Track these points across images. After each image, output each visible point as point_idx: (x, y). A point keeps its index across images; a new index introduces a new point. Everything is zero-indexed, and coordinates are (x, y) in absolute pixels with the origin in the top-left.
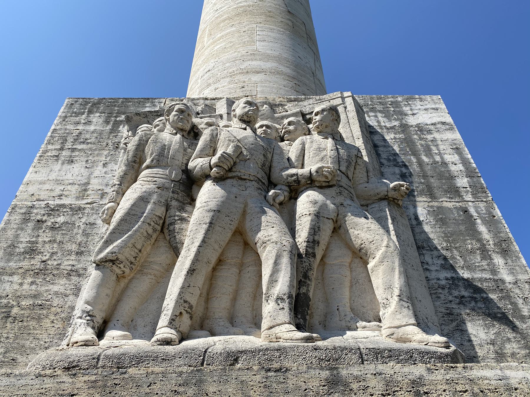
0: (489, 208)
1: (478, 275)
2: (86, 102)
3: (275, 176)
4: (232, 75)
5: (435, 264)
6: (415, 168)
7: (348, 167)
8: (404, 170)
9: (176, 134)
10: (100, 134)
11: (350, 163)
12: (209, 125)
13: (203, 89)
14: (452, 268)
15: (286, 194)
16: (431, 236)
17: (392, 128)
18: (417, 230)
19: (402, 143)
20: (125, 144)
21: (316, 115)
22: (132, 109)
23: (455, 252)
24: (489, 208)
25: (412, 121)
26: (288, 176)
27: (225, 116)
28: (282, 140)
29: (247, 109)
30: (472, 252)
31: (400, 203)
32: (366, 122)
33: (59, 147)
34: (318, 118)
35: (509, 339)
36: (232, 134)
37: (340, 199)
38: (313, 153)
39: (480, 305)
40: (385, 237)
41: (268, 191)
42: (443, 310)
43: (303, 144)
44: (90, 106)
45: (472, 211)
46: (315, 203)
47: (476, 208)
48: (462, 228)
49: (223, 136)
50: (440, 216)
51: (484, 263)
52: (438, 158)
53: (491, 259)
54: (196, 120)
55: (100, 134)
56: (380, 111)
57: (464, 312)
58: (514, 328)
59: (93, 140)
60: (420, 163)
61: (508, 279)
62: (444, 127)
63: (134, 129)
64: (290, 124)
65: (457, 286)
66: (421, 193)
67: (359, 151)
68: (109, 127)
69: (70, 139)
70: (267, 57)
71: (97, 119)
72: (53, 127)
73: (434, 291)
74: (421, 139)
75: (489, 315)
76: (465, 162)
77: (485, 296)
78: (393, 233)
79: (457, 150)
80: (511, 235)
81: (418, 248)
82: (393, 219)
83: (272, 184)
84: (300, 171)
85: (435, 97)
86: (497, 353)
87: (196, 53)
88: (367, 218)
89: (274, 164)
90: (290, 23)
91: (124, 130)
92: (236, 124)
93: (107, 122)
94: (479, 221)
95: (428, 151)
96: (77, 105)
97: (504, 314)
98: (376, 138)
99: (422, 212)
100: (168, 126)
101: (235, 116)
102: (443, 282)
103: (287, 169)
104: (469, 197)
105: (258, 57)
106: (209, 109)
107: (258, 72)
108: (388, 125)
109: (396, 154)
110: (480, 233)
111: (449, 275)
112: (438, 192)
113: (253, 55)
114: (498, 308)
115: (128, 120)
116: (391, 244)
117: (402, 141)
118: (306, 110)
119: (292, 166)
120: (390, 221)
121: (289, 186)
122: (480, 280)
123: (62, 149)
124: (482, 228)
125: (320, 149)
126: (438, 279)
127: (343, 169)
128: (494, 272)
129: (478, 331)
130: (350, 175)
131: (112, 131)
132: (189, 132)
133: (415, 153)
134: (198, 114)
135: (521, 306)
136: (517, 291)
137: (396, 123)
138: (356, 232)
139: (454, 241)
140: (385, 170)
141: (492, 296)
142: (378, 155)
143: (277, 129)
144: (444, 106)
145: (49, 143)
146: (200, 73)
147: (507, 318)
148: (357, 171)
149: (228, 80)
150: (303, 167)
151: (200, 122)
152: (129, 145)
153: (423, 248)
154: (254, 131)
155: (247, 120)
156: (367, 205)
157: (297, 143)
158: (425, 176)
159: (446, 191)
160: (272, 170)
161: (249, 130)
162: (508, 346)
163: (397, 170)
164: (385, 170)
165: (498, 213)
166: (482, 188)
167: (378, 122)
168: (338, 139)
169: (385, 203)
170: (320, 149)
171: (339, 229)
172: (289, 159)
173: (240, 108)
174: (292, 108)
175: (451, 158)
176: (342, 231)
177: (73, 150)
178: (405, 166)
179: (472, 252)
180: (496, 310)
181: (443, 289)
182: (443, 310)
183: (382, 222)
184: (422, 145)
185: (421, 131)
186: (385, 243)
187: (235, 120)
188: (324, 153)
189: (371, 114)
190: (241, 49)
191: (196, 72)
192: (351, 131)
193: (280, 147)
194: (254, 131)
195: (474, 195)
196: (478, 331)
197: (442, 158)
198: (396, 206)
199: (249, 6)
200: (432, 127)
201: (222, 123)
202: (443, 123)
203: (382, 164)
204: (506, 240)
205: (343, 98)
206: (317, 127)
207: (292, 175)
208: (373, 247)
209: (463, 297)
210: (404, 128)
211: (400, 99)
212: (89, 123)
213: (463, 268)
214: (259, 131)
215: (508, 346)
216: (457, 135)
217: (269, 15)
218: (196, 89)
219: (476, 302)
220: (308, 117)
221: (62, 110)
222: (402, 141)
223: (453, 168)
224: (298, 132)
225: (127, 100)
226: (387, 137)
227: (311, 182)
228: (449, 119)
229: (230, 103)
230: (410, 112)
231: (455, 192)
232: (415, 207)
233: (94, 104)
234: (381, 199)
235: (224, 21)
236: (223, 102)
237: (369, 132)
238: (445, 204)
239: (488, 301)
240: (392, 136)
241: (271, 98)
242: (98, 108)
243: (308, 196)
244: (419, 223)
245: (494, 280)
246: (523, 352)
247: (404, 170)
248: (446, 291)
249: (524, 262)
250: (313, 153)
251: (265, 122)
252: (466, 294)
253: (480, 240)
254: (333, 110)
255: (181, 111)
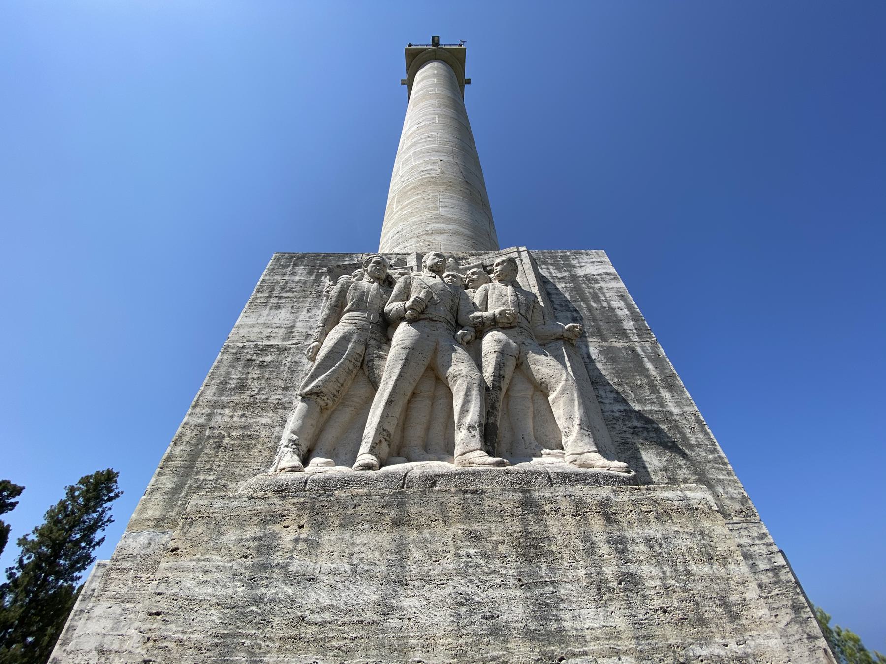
0: (654, 348)
1: (648, 408)
2: (291, 256)
3: (461, 320)
4: (418, 235)
5: (609, 398)
6: (585, 312)
7: (527, 311)
8: (575, 314)
9: (373, 282)
10: (305, 284)
11: (528, 308)
12: (402, 274)
13: (393, 248)
14: (625, 401)
15: (472, 334)
16: (604, 372)
17: (562, 278)
18: (590, 367)
19: (572, 291)
20: (327, 292)
21: (497, 265)
22: (333, 263)
23: (626, 387)
24: (654, 348)
25: (580, 272)
26: (474, 318)
27: (415, 268)
28: (467, 288)
29: (436, 261)
30: (642, 387)
31: (574, 342)
32: (539, 273)
33: (267, 295)
34: (499, 268)
35: (680, 466)
36: (423, 281)
37: (521, 339)
38: (495, 298)
39: (652, 434)
40: (564, 372)
41: (457, 332)
42: (619, 440)
43: (486, 291)
44: (295, 260)
45: (639, 350)
46: (499, 341)
47: (642, 347)
48: (631, 365)
49: (415, 284)
50: (610, 355)
51: (653, 397)
52: (605, 304)
53: (659, 393)
54: (390, 271)
55: (305, 284)
56: (551, 264)
57: (638, 441)
58: (684, 456)
59: (298, 289)
60: (589, 308)
61: (676, 411)
62: (609, 277)
63: (335, 280)
64: (473, 274)
65: (631, 417)
66: (592, 335)
67: (536, 296)
68: (313, 278)
69: (277, 288)
70: (447, 220)
71: (301, 273)
72: (262, 278)
73: (610, 422)
74: (589, 287)
75: (660, 444)
76: (629, 307)
77: (656, 426)
78: (569, 369)
79: (622, 297)
80: (675, 372)
81: (592, 383)
82: (569, 357)
83: (459, 326)
84: (485, 314)
85: (599, 252)
86: (669, 478)
87: (386, 217)
88: (546, 355)
89: (461, 308)
90: (468, 192)
91: (326, 281)
92: (426, 274)
93: (310, 274)
94: (646, 359)
95: (596, 299)
96: (283, 259)
97: (674, 442)
98: (549, 287)
99: (593, 351)
100: (366, 276)
101: (425, 266)
102: (617, 414)
103: (473, 312)
104: (635, 338)
105: (441, 221)
106: (401, 262)
107: (441, 233)
108: (559, 276)
109: (567, 301)
110: (648, 370)
111: (622, 408)
112: (607, 334)
113: (438, 219)
114: (668, 437)
115: (330, 272)
116: (570, 378)
117: (571, 290)
118: (487, 262)
119: (476, 309)
120: (566, 358)
121: (475, 328)
122: (651, 412)
123: (270, 297)
124: (649, 366)
125: (501, 295)
126: (613, 411)
127: (523, 312)
128: (663, 404)
129: (651, 458)
130: (529, 317)
131: (315, 281)
132: (385, 281)
133: (585, 300)
134: (391, 266)
135: (689, 435)
136: (684, 422)
137: (566, 274)
138: (537, 368)
139: (625, 377)
140: (558, 314)
141: (662, 427)
142: (552, 302)
143: (462, 279)
144: (608, 259)
145: (258, 291)
146: (390, 234)
147: (677, 447)
148: (535, 315)
149: (415, 239)
150: (486, 310)
151: (394, 272)
152: (331, 293)
153: (597, 383)
154: (442, 279)
155: (436, 270)
156: (548, 343)
157: (481, 289)
158: (594, 320)
159: (614, 333)
160: (459, 313)
161: (438, 278)
162: (679, 472)
163: (569, 315)
164: (558, 314)
165: (662, 351)
166: (647, 330)
167: (550, 273)
168: (516, 286)
169: (561, 342)
170: (501, 295)
171: (521, 365)
172: (474, 304)
173: (429, 260)
174: (474, 261)
175: (617, 304)
176: (523, 367)
177: (280, 297)
178: (576, 311)
179: (642, 387)
180: (666, 440)
181: (617, 420)
182: (619, 440)
183: (559, 359)
184: (590, 293)
185: (589, 280)
186: (564, 377)
187: (425, 270)
188: (506, 298)
189: (543, 266)
190: (426, 214)
191: (386, 234)
192: (527, 280)
193: (465, 293)
194: (442, 279)
195: (640, 336)
196: (651, 458)
197: (609, 304)
198: (570, 345)
199: (432, 177)
200: (598, 277)
201: (413, 274)
202: (608, 274)
203: (555, 309)
204: (672, 376)
205: (519, 252)
206: (498, 276)
207: (478, 317)
208: (553, 381)
209: (636, 427)
210: (574, 278)
211: (568, 254)
212: (294, 274)
213: (634, 401)
214: (446, 280)
215: (679, 472)
216: (621, 285)
217: (450, 185)
218: (386, 246)
219: (648, 432)
220: (488, 268)
221: (270, 263)
222: (571, 290)
223: (619, 313)
224: (481, 281)
225: (328, 255)
226: (559, 286)
227: (494, 323)
228: (613, 271)
229: (420, 257)
230: (578, 265)
231: (623, 334)
232: (587, 347)
233: (299, 258)
234: (557, 339)
235: (410, 190)
236: (414, 256)
237: (542, 282)
238: (614, 344)
239: (658, 431)
240: (563, 285)
241: (454, 253)
242: (302, 261)
243: (493, 336)
244: (592, 361)
245: (663, 412)
246: (693, 478)
247: (575, 314)
248: (620, 422)
249: (689, 396)
250: (495, 298)
251: (451, 273)
252: (638, 425)
253: (648, 376)
254: (512, 261)
255: (377, 263)
